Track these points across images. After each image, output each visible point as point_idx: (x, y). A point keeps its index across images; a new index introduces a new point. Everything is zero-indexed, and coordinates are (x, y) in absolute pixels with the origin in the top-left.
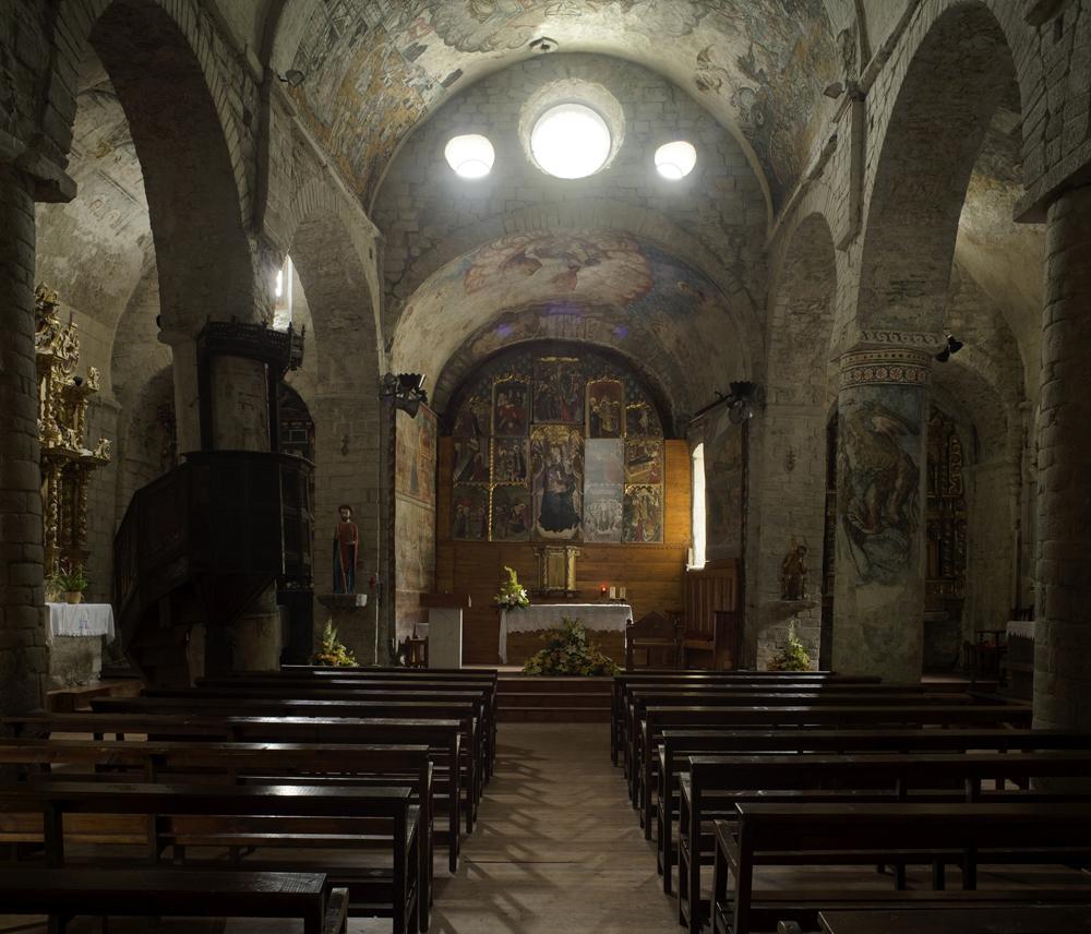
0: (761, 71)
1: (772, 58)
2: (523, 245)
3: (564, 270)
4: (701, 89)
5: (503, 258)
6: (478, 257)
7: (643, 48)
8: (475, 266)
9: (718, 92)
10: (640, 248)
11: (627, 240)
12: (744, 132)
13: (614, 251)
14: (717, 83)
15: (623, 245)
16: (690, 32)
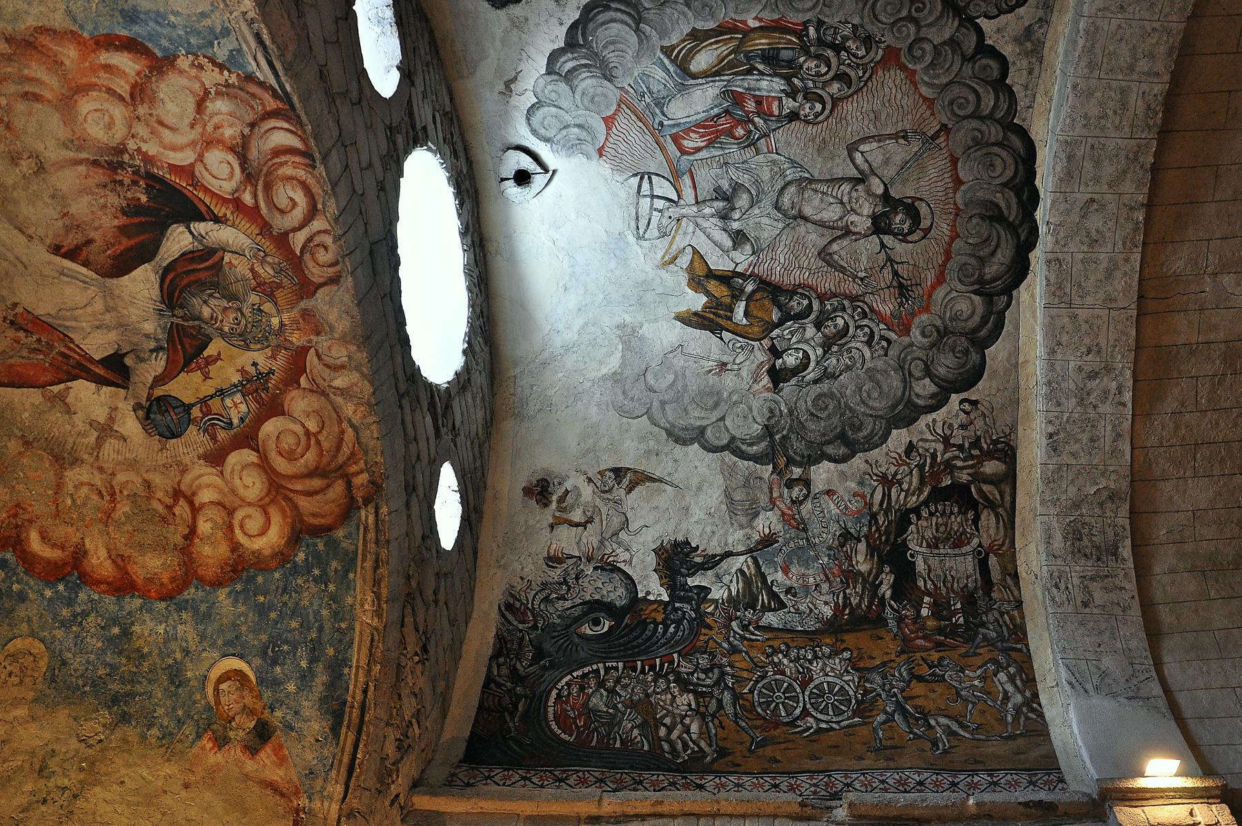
0: (706, 590)
1: (764, 597)
2: (253, 213)
3: (98, 345)
4: (527, 491)
5: (184, 158)
6: (212, 77)
7: (570, 361)
8: (161, 64)
9: (552, 527)
10: (329, 528)
11: (338, 488)
12: (509, 606)
13: (264, 465)
14: (577, 516)
15: (317, 483)
16: (682, 441)
